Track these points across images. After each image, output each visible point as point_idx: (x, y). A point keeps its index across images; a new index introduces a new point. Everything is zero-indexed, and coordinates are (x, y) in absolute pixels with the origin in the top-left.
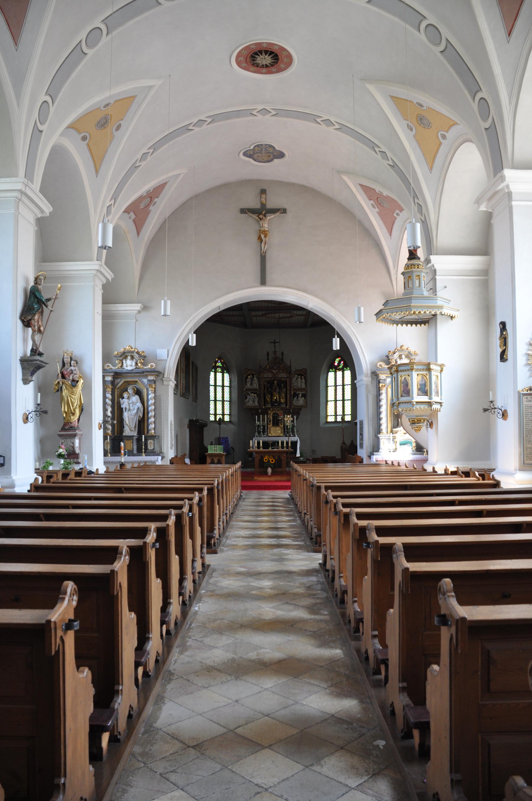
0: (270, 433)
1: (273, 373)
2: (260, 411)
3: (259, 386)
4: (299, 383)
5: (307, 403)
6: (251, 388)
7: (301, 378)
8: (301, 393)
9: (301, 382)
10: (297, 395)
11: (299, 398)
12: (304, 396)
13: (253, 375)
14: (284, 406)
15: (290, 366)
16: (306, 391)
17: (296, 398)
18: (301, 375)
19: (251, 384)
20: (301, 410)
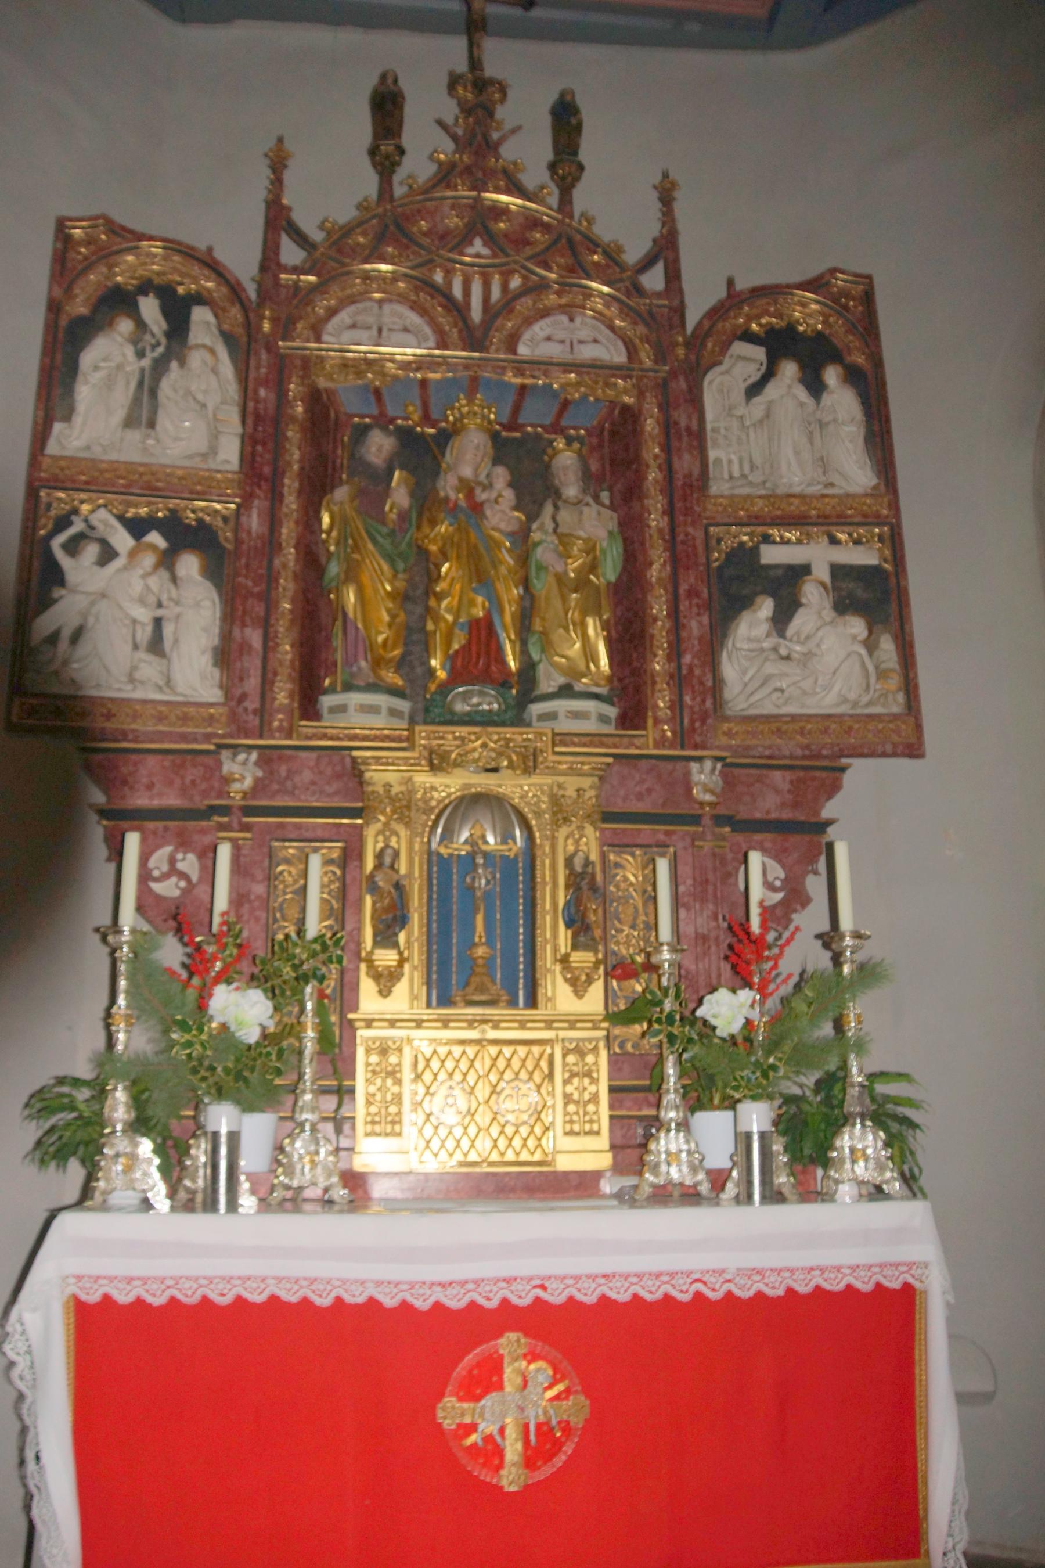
0: (389, 1124)
1: (459, 310)
2: (242, 772)
3: (250, 443)
4: (771, 439)
5: (910, 688)
6: (132, 449)
7: (815, 387)
8: (819, 556)
9: (818, 427)
10: (786, 586)
11: (802, 622)
12: (876, 597)
13: (177, 311)
14: (591, 716)
15: (666, 249)
16: (895, 541)
17: (754, 623)
18: (805, 353)
19: (144, 410)
20: (833, 788)
